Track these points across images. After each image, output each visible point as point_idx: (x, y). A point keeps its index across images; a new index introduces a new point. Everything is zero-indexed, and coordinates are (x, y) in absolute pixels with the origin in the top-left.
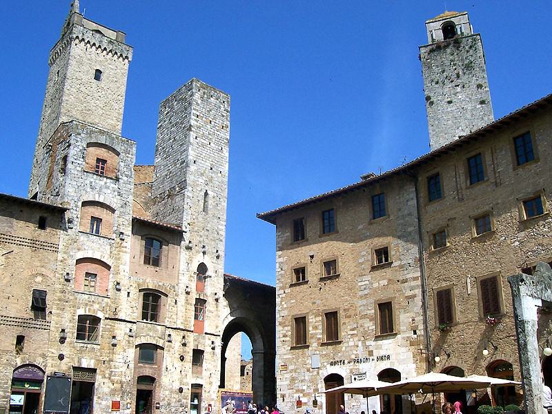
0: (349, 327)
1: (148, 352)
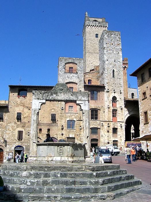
1: (94, 130)
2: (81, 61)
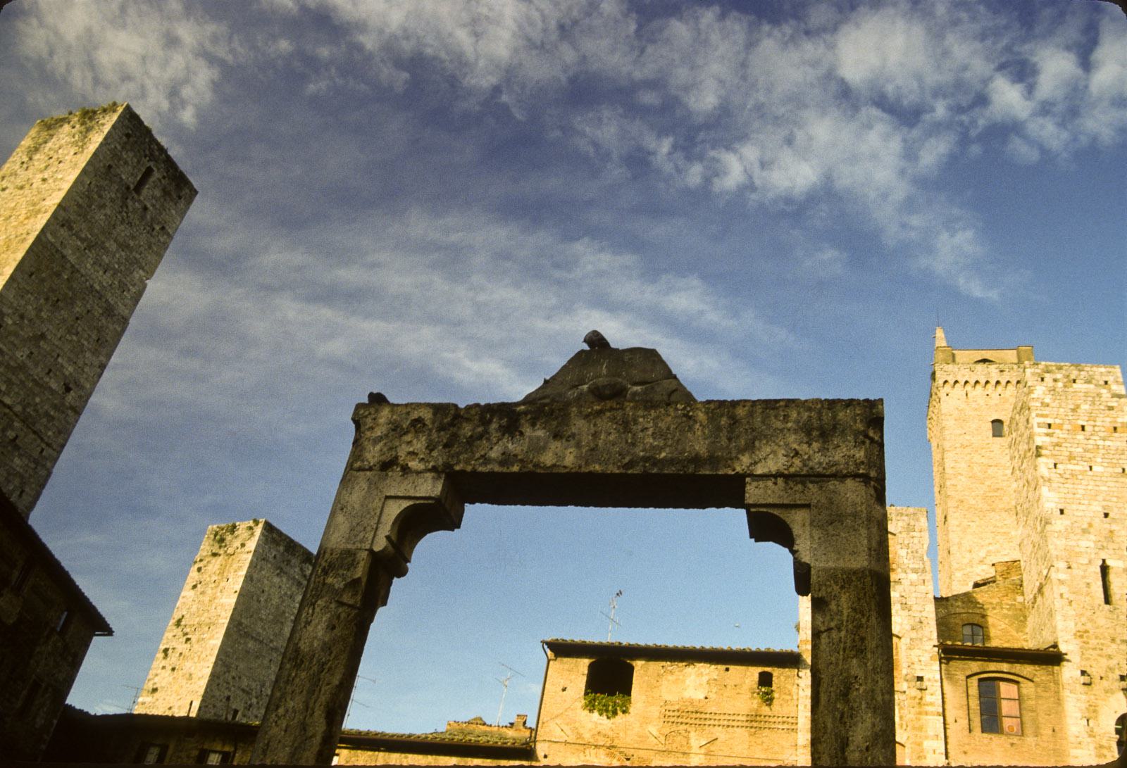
2: (918, 520)
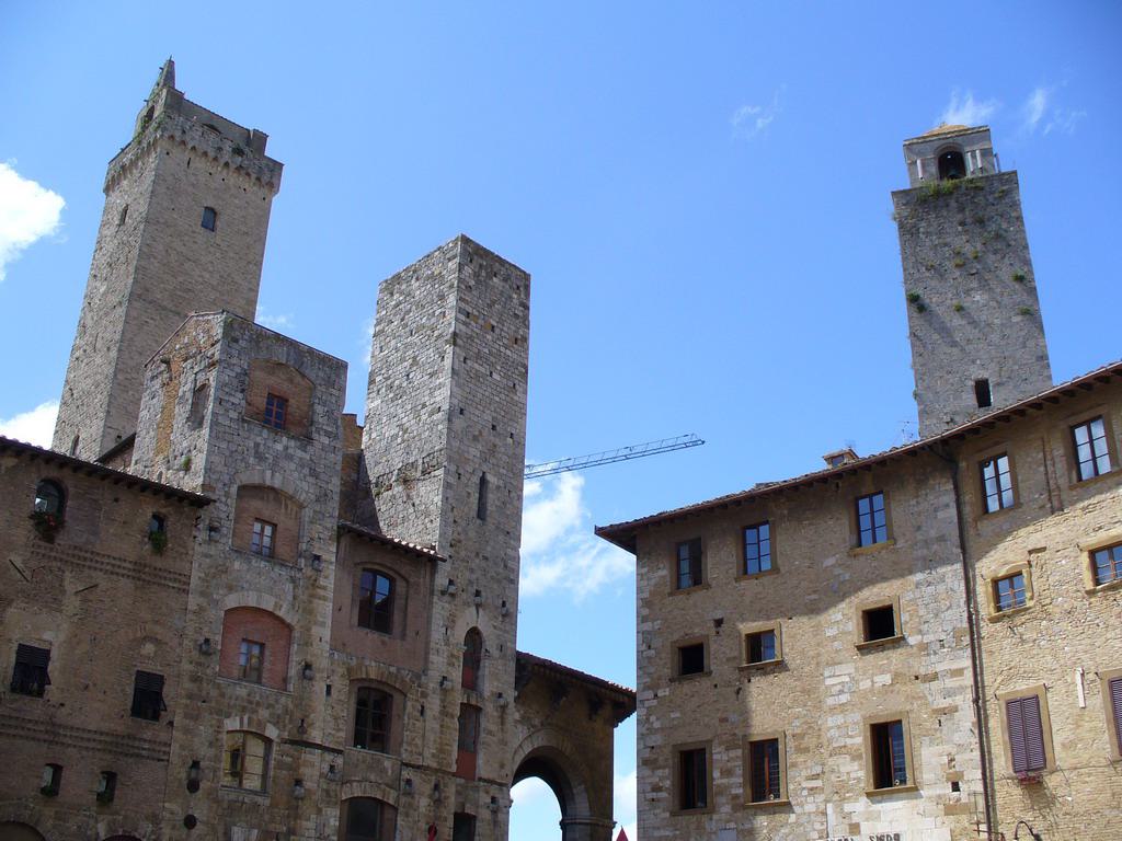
0: (804, 773)
